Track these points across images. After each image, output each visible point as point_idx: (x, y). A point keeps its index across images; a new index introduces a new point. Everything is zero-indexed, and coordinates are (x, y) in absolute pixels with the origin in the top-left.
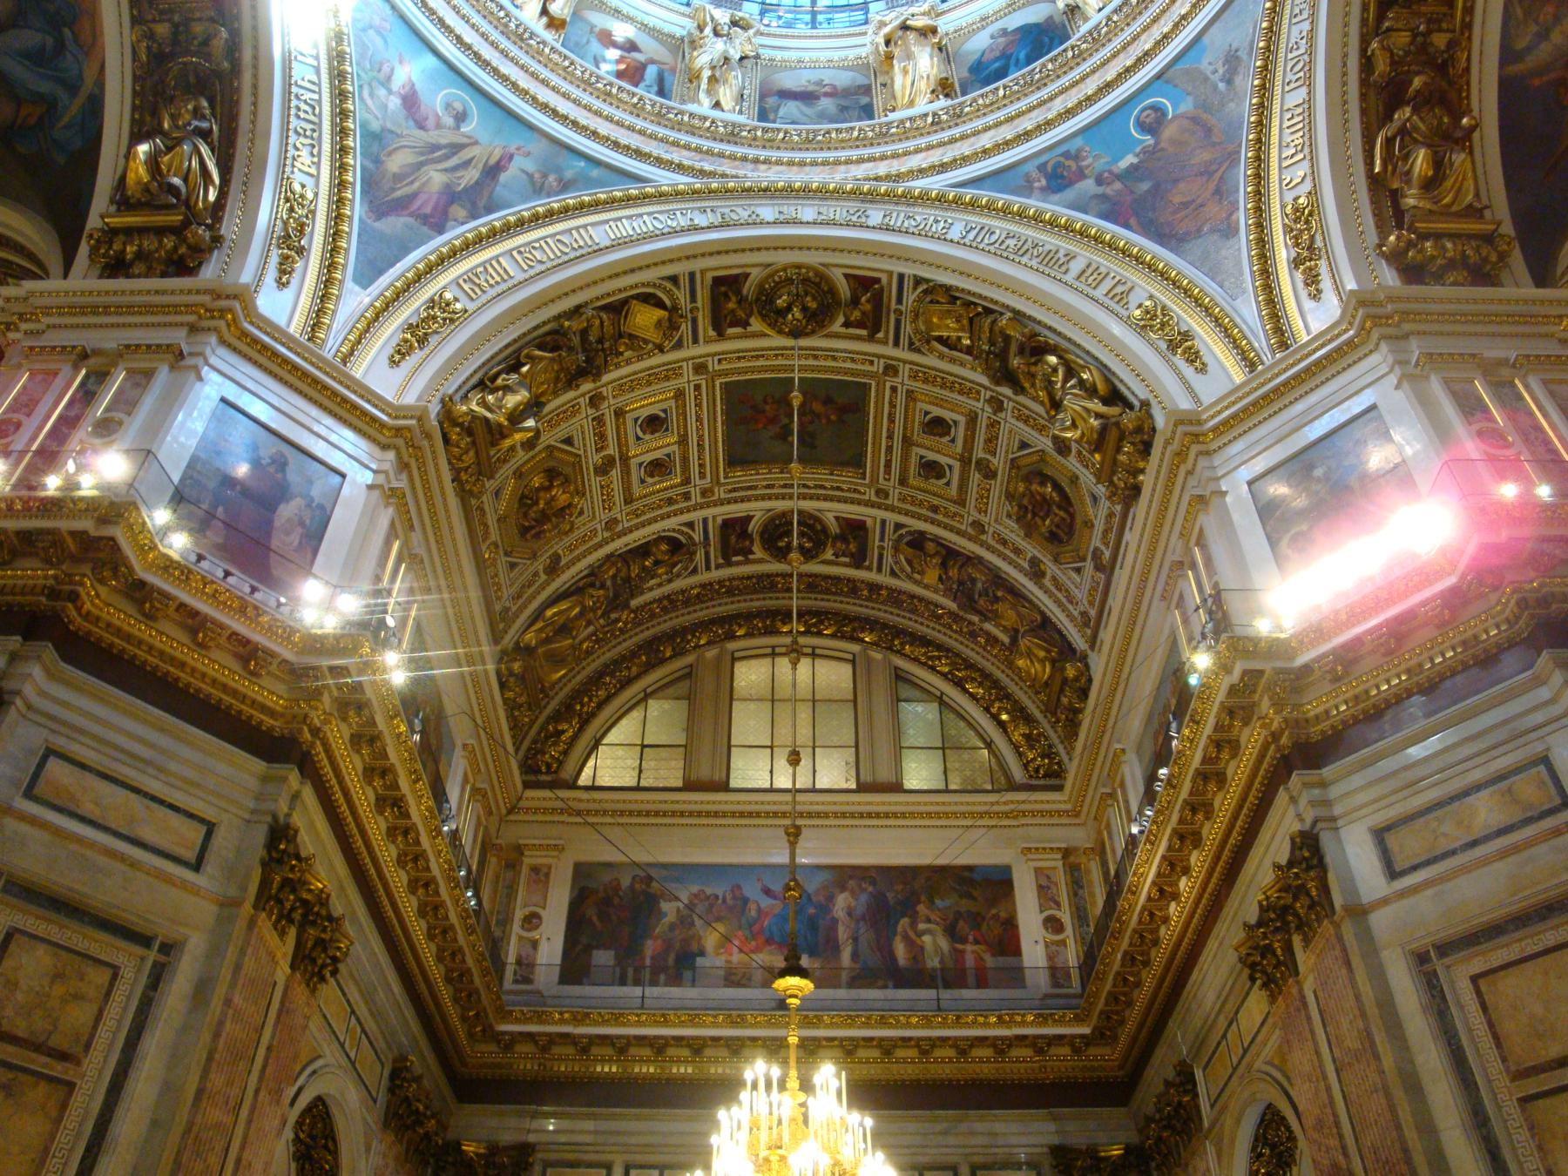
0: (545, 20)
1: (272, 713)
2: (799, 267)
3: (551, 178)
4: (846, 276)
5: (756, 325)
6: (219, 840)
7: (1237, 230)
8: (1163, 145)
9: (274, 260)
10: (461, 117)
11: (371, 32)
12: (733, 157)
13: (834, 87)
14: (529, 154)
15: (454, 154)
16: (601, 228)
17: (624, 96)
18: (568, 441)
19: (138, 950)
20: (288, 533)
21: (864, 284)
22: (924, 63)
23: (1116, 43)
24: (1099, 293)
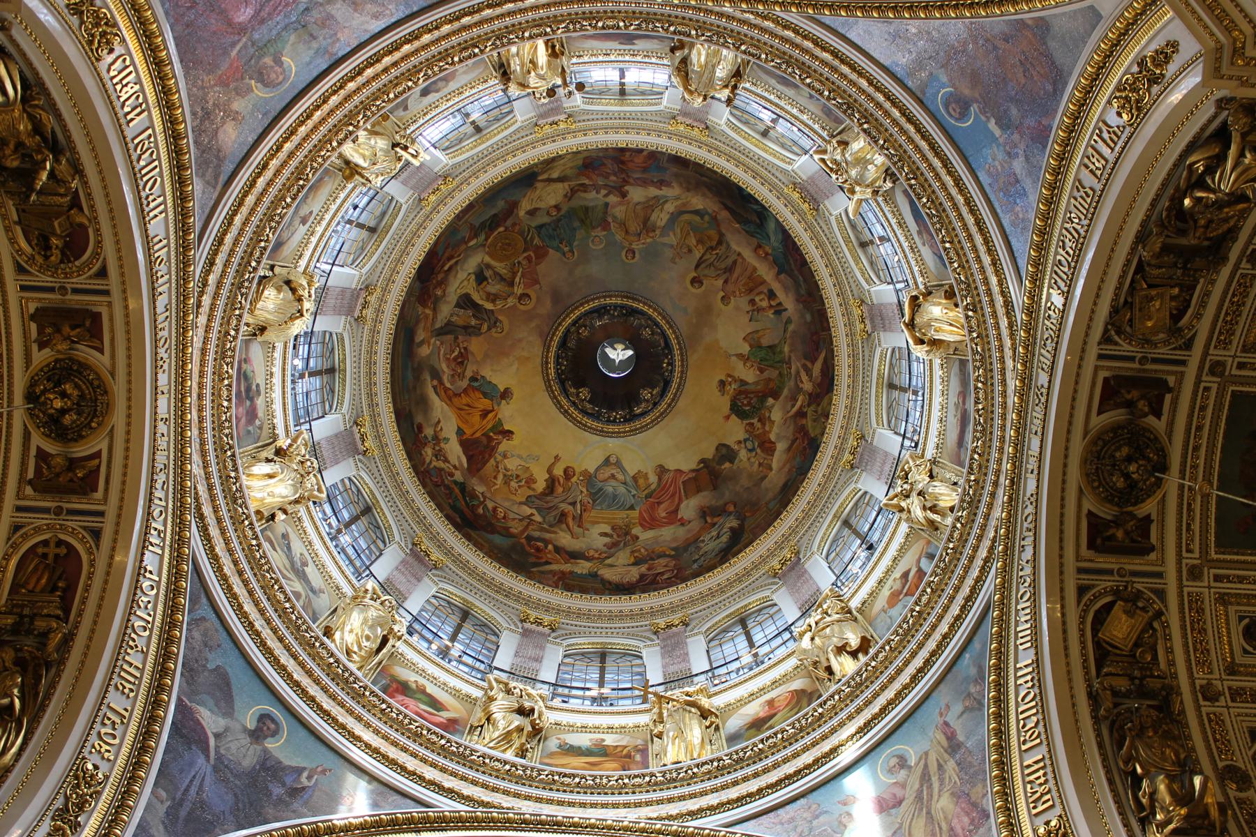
0: (860, 655)
2: (1084, 462)
3: (973, 690)
4: (1099, 413)
5: (1148, 507)
7: (1041, 18)
8: (977, 95)
10: (902, 762)
11: (815, 823)
12: (990, 506)
13: (960, 393)
14: (948, 707)
15: (930, 779)
16: (1021, 654)
17: (925, 599)
21: (1112, 392)
22: (936, 310)
23: (902, 139)
24: (1111, 158)
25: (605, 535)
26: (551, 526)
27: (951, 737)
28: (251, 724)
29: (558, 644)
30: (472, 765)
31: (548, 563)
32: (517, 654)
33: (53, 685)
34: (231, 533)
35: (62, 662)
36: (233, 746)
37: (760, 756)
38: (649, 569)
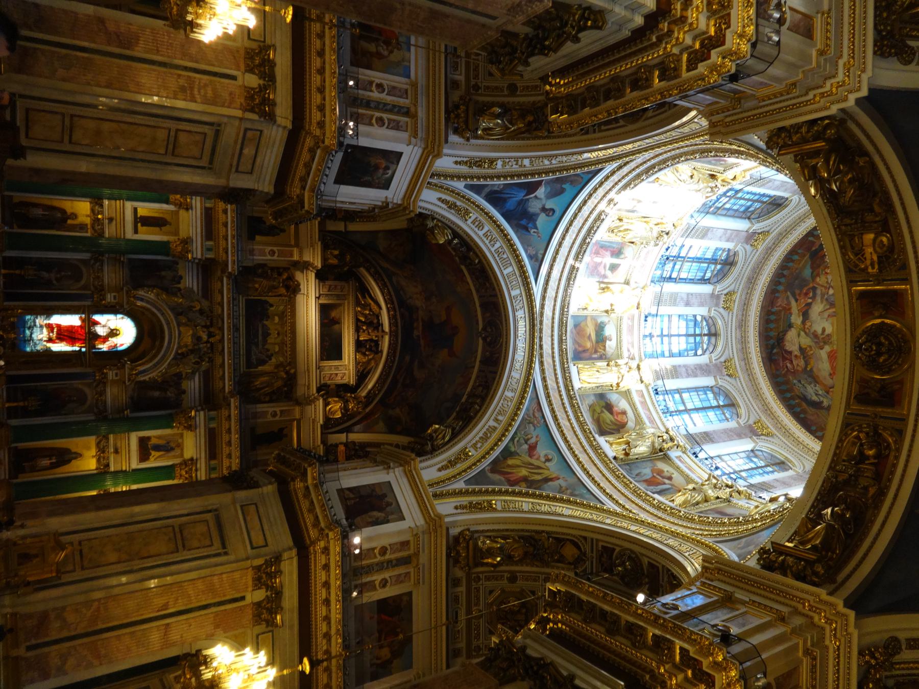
1: (310, 539)
2: (632, 551)
3: (569, 491)
6: (263, 549)
9: (443, 464)
10: (548, 460)
18: (533, 593)
19: (220, 546)
20: (370, 517)
25: (824, 330)
26: (827, 300)
27: (551, 480)
28: (547, 207)
29: (709, 311)
30: (566, 290)
31: (796, 300)
32: (688, 294)
33: (523, 139)
34: (631, 176)
35: (534, 139)
36: (535, 203)
37: (572, 406)
38: (796, 356)
